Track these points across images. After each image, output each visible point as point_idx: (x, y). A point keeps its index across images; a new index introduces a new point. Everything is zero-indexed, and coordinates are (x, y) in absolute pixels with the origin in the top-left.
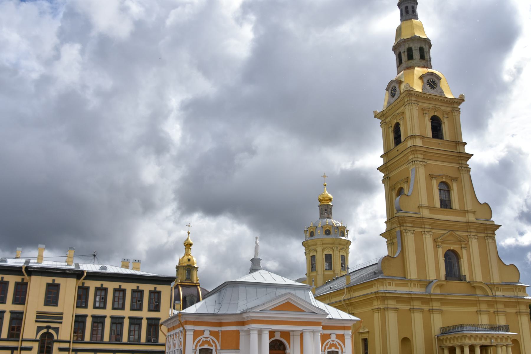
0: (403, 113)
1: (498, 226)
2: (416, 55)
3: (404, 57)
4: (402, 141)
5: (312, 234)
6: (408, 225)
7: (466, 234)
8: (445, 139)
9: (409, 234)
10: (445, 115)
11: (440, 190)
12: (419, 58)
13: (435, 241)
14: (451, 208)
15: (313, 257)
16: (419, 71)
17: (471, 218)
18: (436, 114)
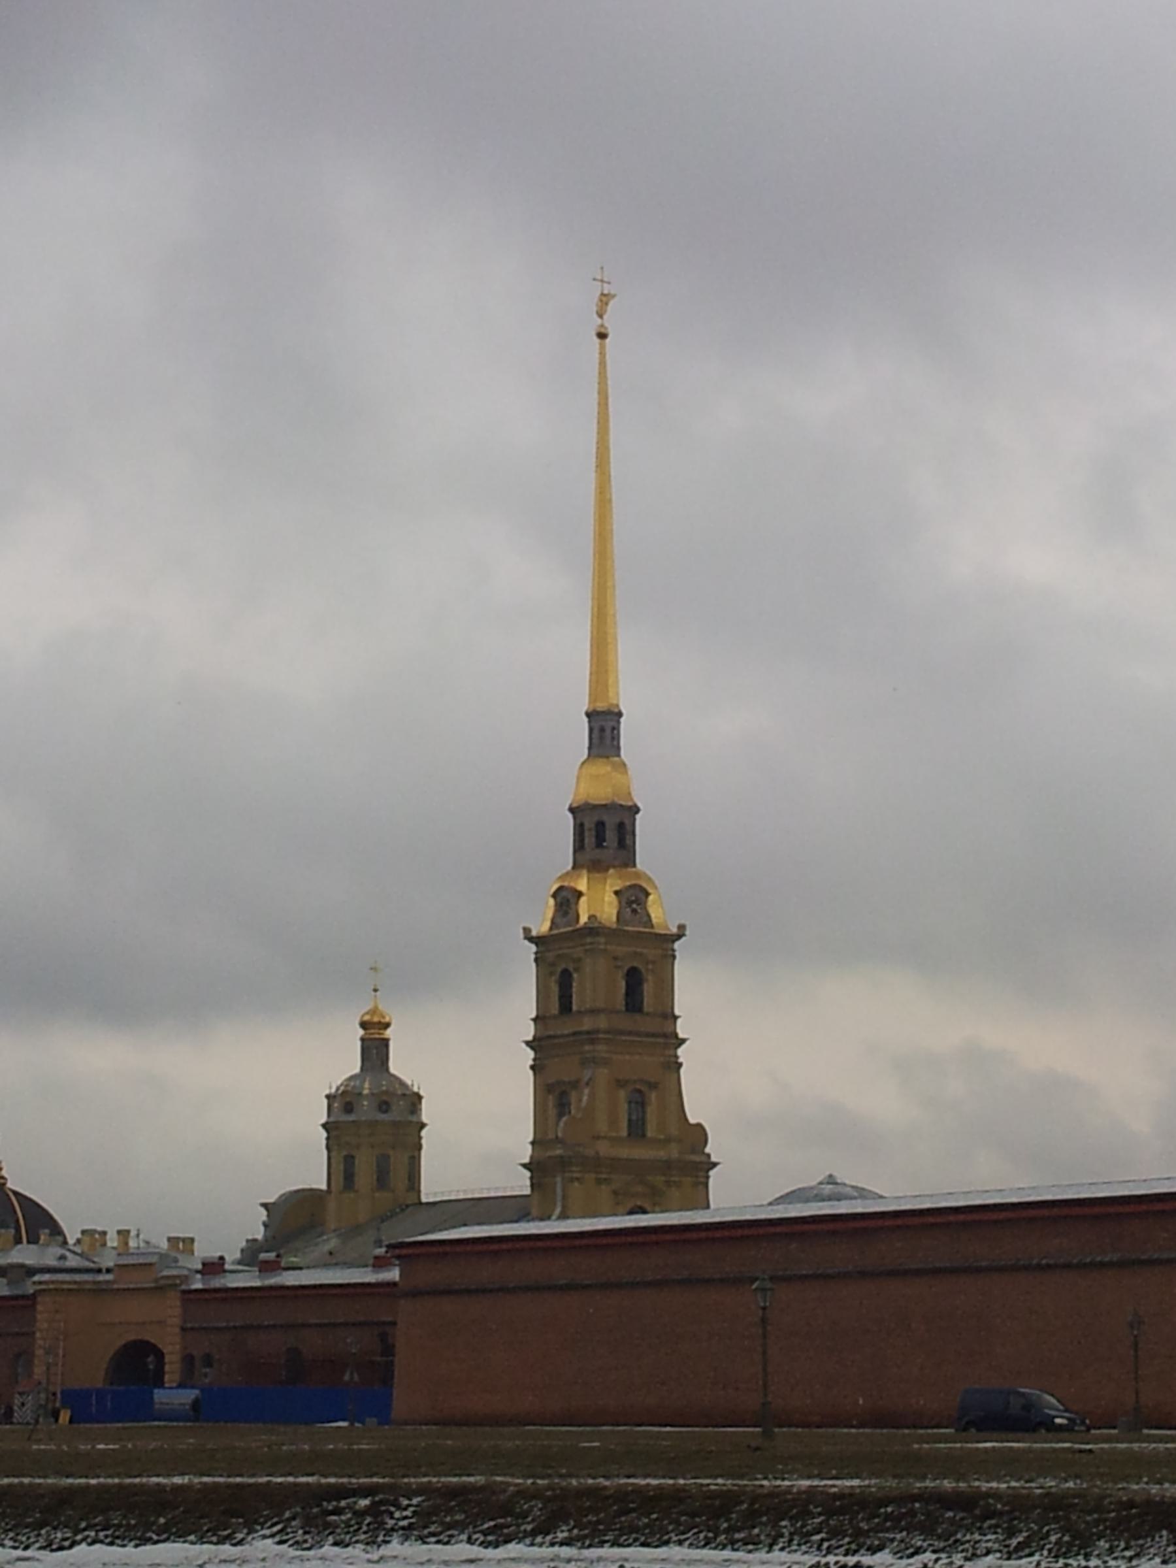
0: (579, 960)
1: (715, 1165)
2: (611, 836)
3: (589, 839)
4: (575, 1008)
5: (348, 1108)
6: (574, 1169)
7: (663, 1178)
8: (646, 1009)
9: (576, 1184)
10: (650, 967)
11: (630, 1102)
12: (616, 844)
13: (615, 1193)
14: (644, 1135)
15: (349, 1160)
16: (613, 882)
17: (674, 1152)
18: (635, 964)
